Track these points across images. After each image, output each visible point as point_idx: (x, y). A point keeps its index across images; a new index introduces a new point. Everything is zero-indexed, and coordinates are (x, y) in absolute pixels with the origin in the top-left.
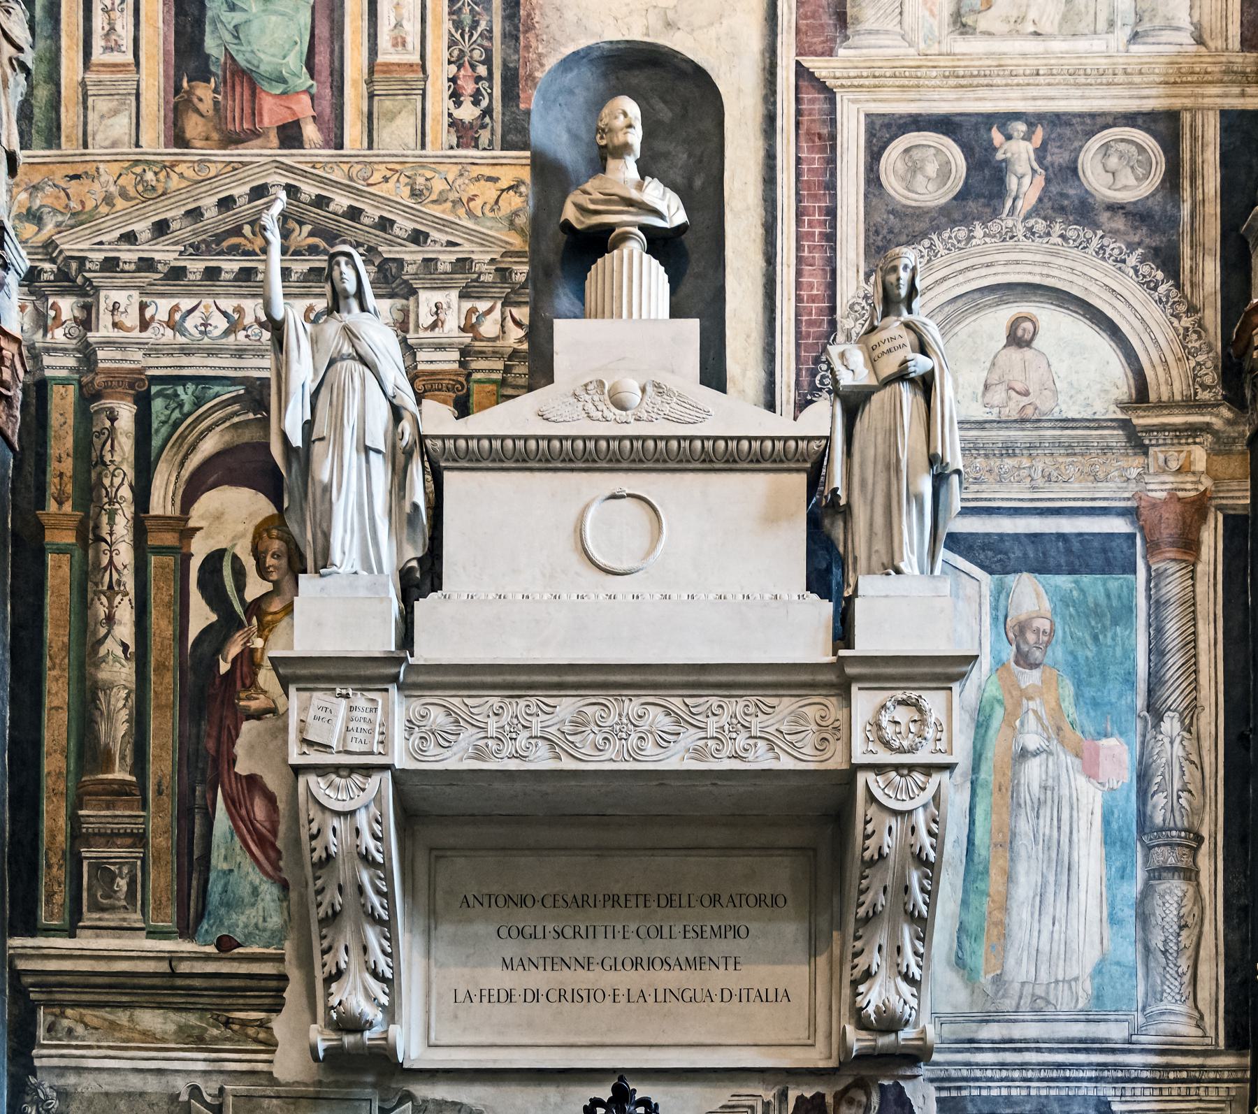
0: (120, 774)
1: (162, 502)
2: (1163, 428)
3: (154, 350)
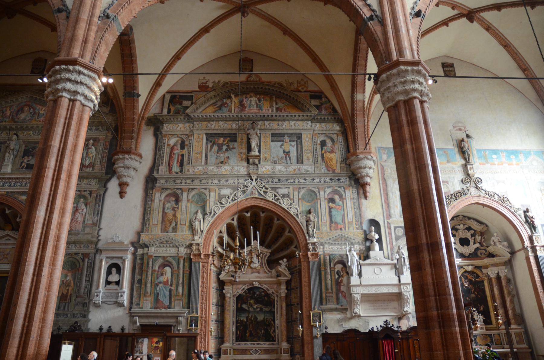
0: (330, 291)
1: (332, 266)
3: (330, 251)
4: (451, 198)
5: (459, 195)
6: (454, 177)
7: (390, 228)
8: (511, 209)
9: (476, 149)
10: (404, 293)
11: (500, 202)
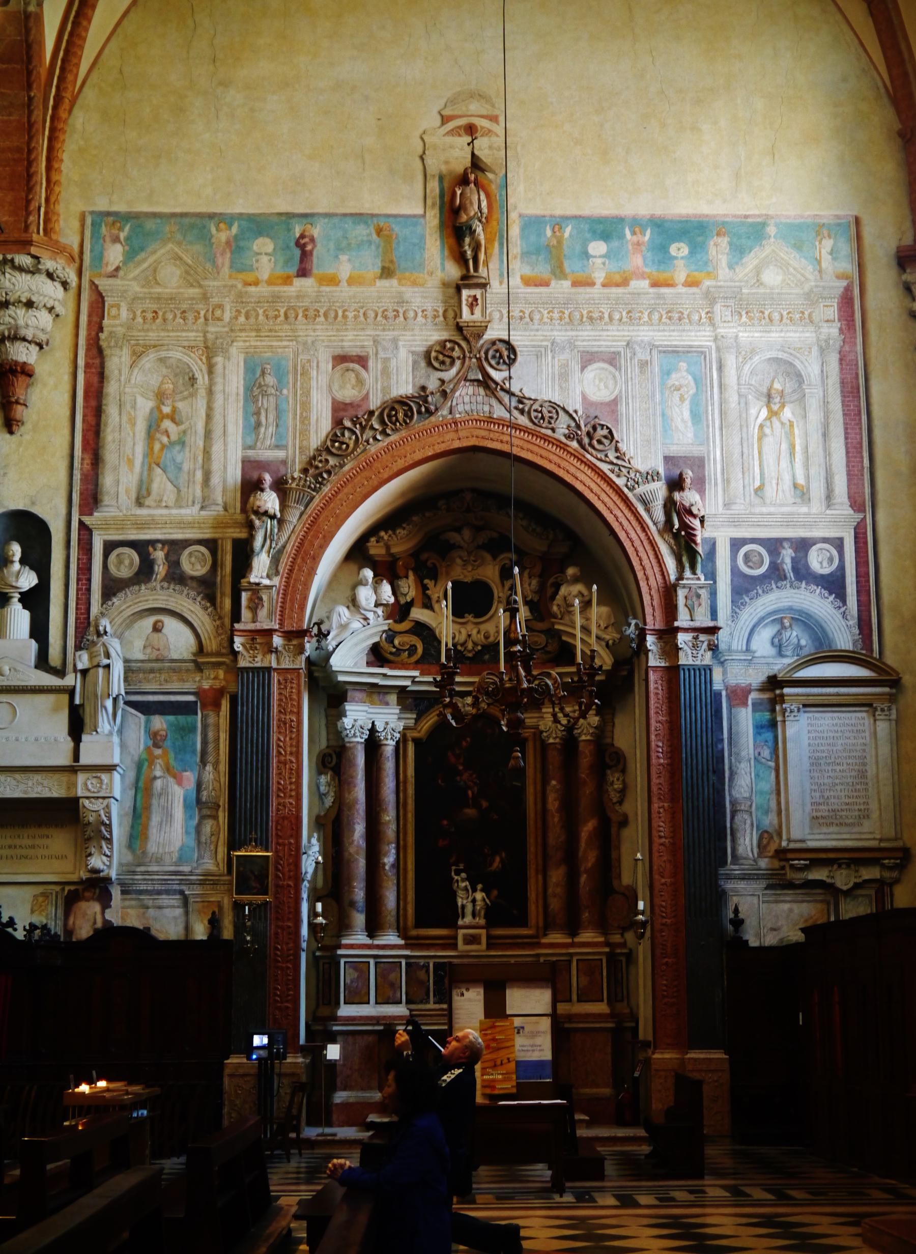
2: (208, 663)
4: (363, 429)
5: (401, 415)
6: (395, 341)
7: (86, 547)
8: (613, 477)
9: (520, 216)
10: (86, 802)
11: (574, 444)
